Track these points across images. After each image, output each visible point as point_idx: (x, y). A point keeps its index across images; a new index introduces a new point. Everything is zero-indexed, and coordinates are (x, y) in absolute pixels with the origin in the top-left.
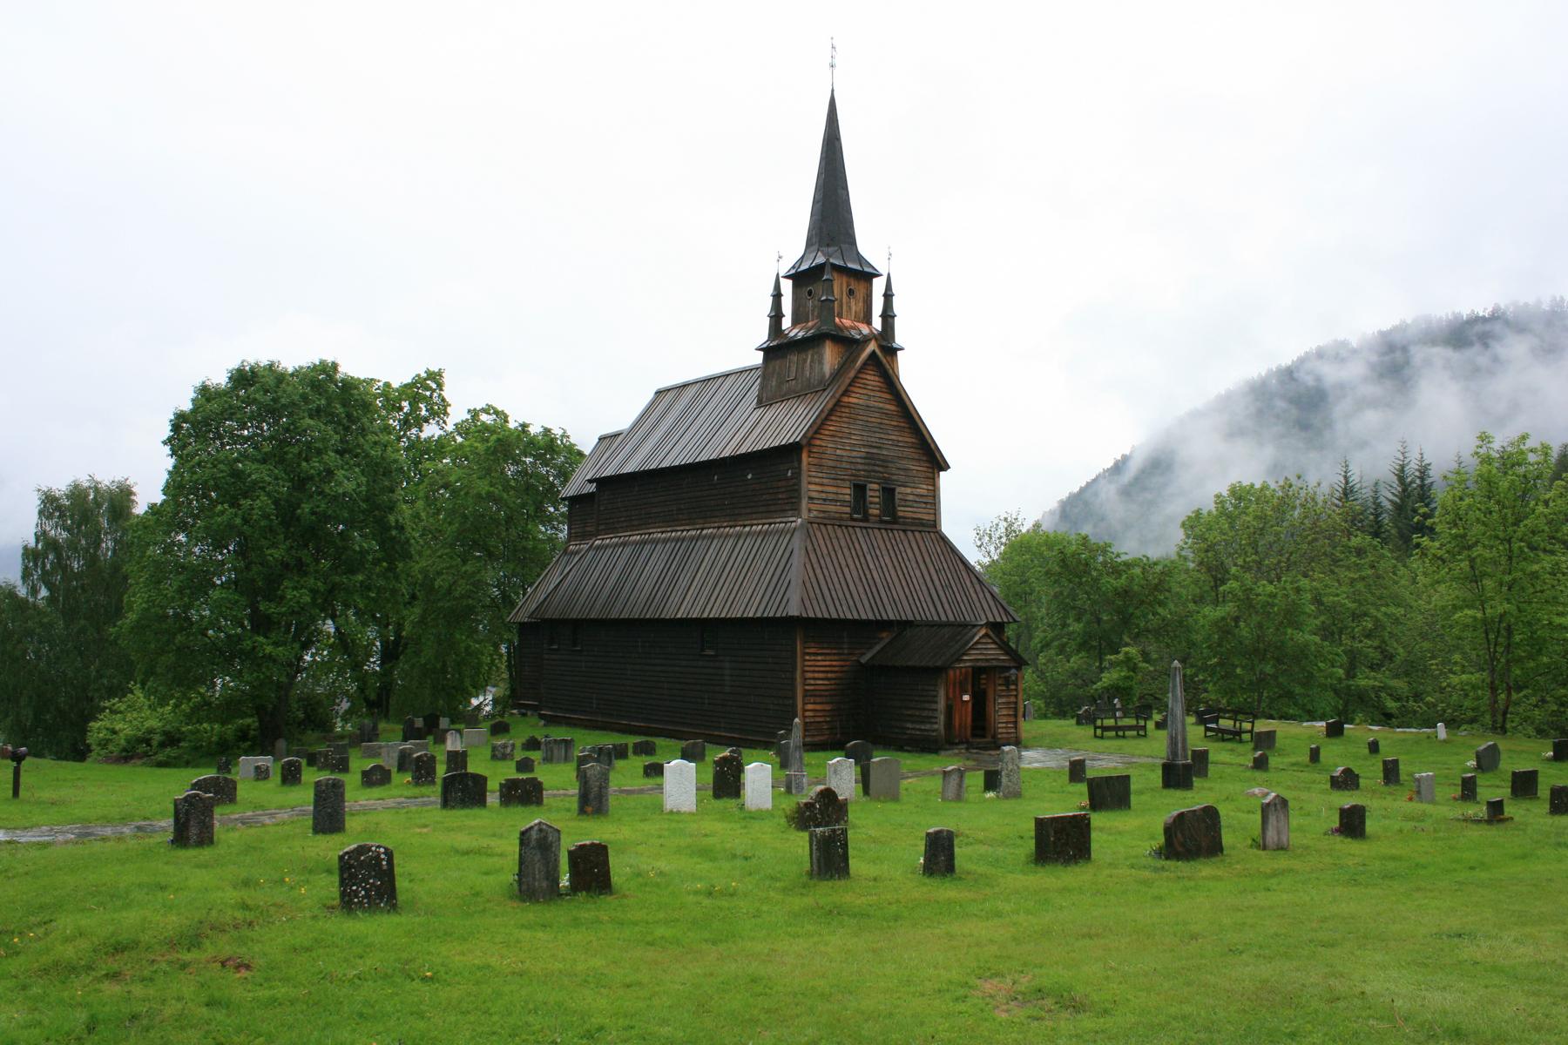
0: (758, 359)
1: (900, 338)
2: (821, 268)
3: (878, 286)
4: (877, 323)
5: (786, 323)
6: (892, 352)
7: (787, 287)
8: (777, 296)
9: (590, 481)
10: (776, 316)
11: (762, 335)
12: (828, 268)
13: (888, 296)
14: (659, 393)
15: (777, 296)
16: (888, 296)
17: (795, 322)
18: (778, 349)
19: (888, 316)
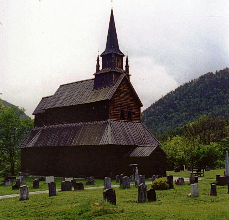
0: (94, 77)
1: (130, 73)
2: (111, 54)
3: (124, 59)
4: (124, 68)
5: (101, 68)
6: (129, 76)
7: (101, 59)
8: (98, 61)
9: (44, 110)
10: (98, 66)
11: (95, 71)
12: (113, 54)
13: (127, 61)
14: (61, 86)
15: (98, 61)
16: (127, 61)
17: (103, 68)
18: (98, 75)
19: (127, 67)
